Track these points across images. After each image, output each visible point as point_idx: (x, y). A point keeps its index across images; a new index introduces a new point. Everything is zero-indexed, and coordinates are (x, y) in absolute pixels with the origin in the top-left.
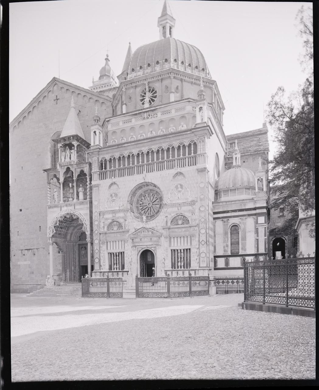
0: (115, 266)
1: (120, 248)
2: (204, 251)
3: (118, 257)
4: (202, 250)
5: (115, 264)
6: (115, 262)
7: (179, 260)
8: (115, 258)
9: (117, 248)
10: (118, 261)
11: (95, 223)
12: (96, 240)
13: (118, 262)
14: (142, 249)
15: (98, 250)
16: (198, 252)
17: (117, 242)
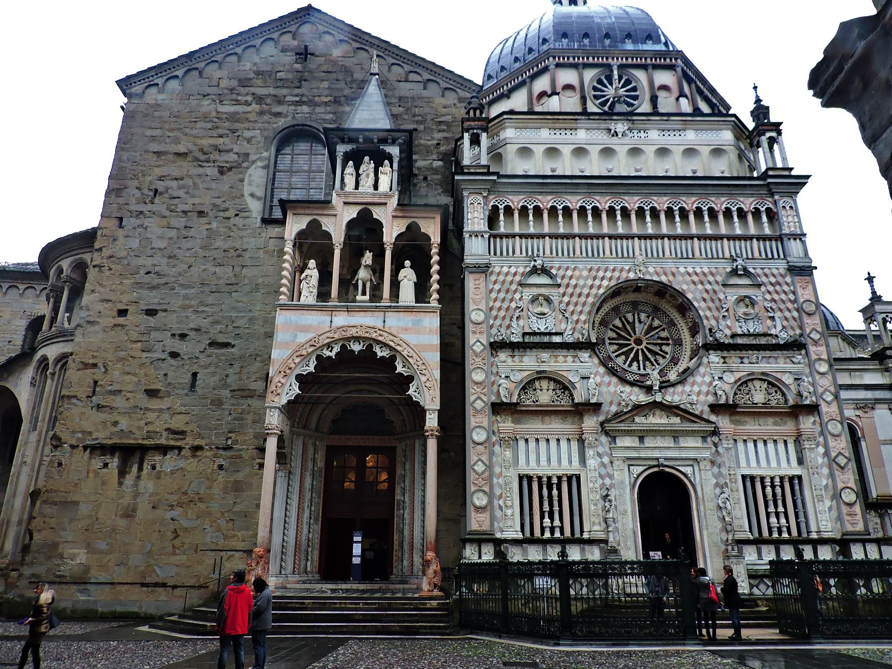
0: (547, 521)
1: (565, 462)
2: (849, 485)
3: (555, 492)
4: (843, 483)
5: (546, 515)
6: (546, 508)
7: (771, 509)
8: (545, 492)
9: (554, 459)
10: (556, 503)
11: (475, 376)
12: (478, 430)
13: (556, 508)
14: (646, 470)
15: (483, 462)
16: (830, 487)
17: (553, 443)
